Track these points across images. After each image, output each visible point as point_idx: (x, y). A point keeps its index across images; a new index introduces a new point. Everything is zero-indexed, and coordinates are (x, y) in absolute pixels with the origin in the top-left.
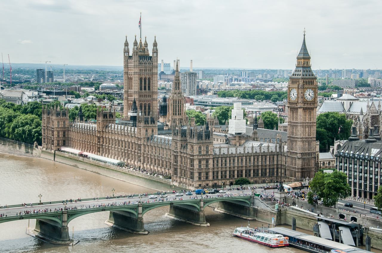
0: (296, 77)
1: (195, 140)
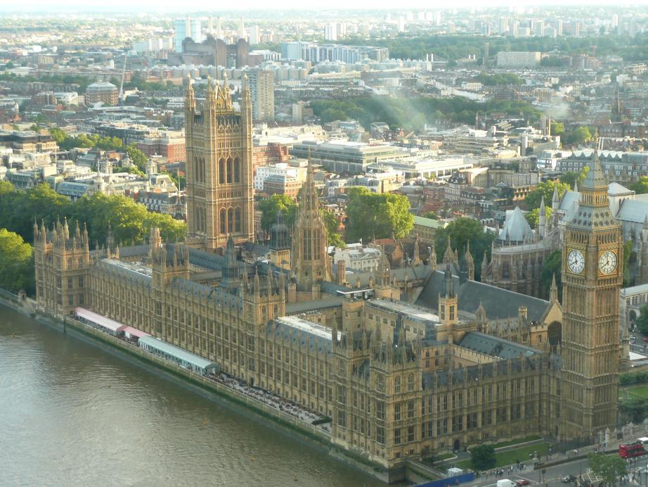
1: (387, 367)
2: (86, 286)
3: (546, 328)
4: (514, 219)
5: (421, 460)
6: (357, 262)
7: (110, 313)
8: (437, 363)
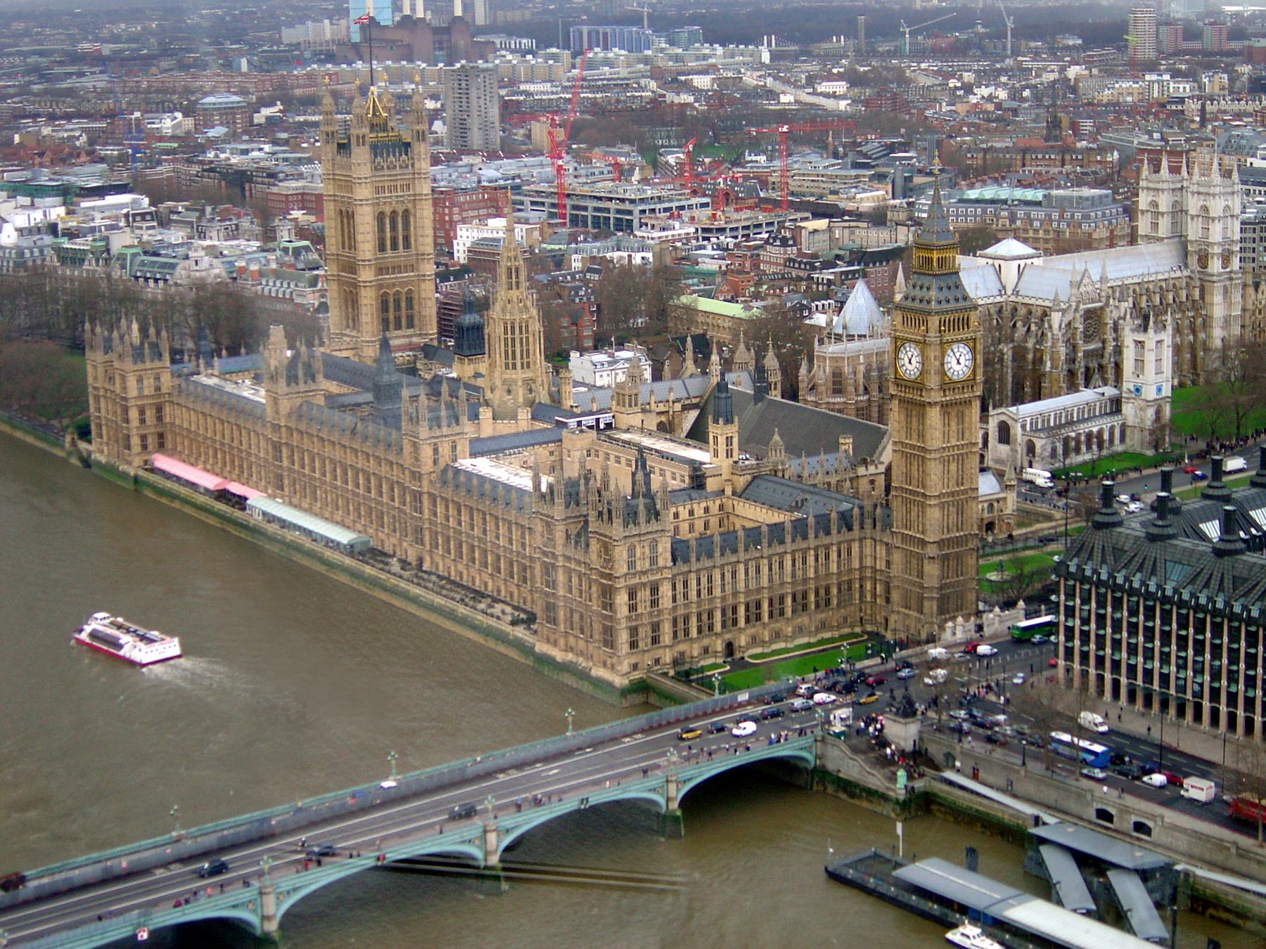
0: (917, 304)
1: (617, 530)
2: (167, 419)
3: (882, 469)
4: (860, 299)
5: (672, 673)
6: (605, 374)
7: (205, 462)
8: (706, 526)
